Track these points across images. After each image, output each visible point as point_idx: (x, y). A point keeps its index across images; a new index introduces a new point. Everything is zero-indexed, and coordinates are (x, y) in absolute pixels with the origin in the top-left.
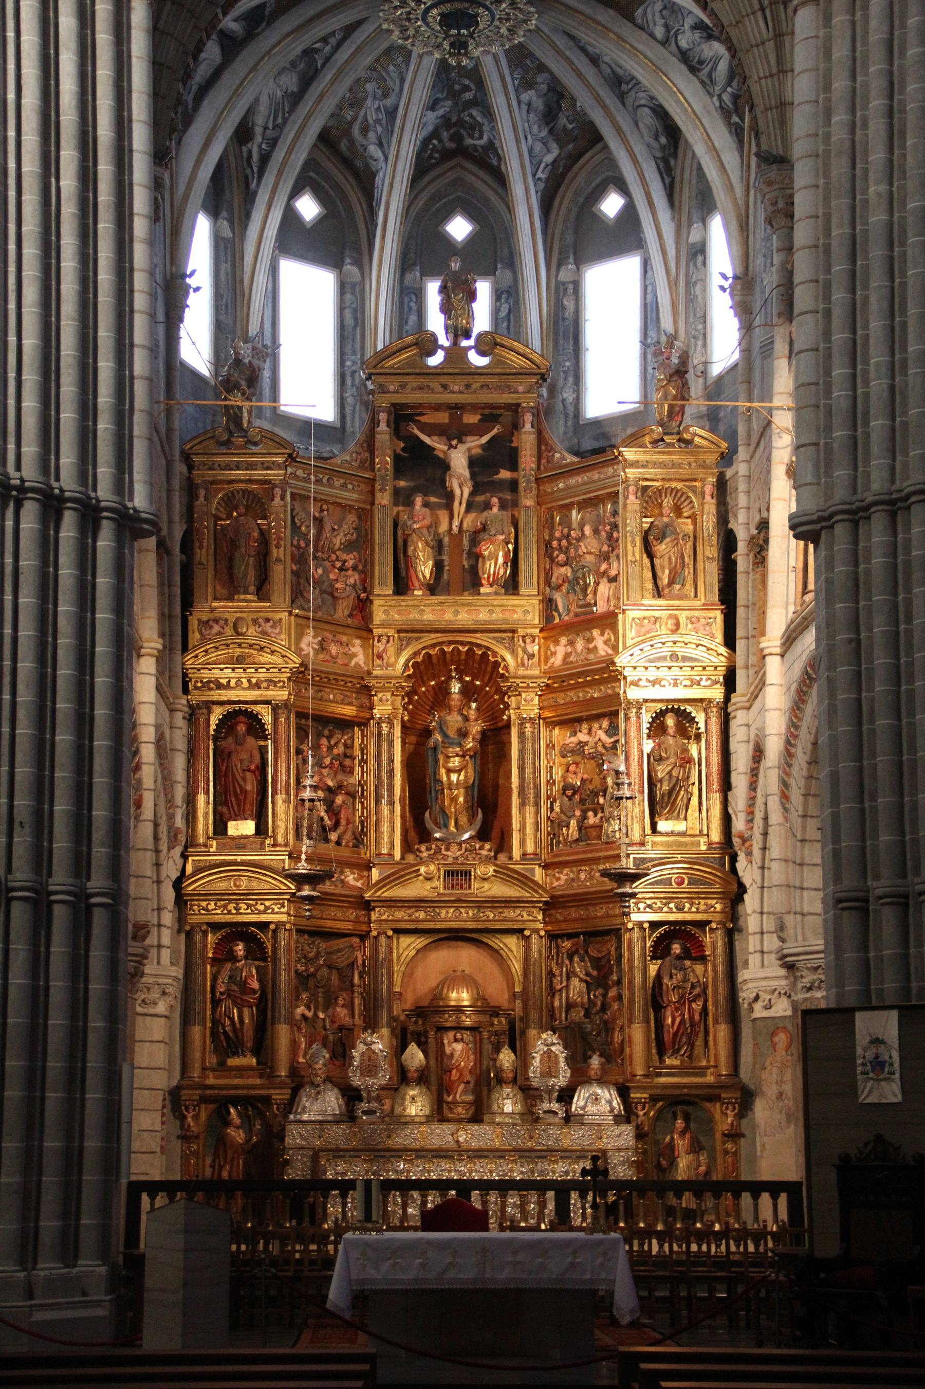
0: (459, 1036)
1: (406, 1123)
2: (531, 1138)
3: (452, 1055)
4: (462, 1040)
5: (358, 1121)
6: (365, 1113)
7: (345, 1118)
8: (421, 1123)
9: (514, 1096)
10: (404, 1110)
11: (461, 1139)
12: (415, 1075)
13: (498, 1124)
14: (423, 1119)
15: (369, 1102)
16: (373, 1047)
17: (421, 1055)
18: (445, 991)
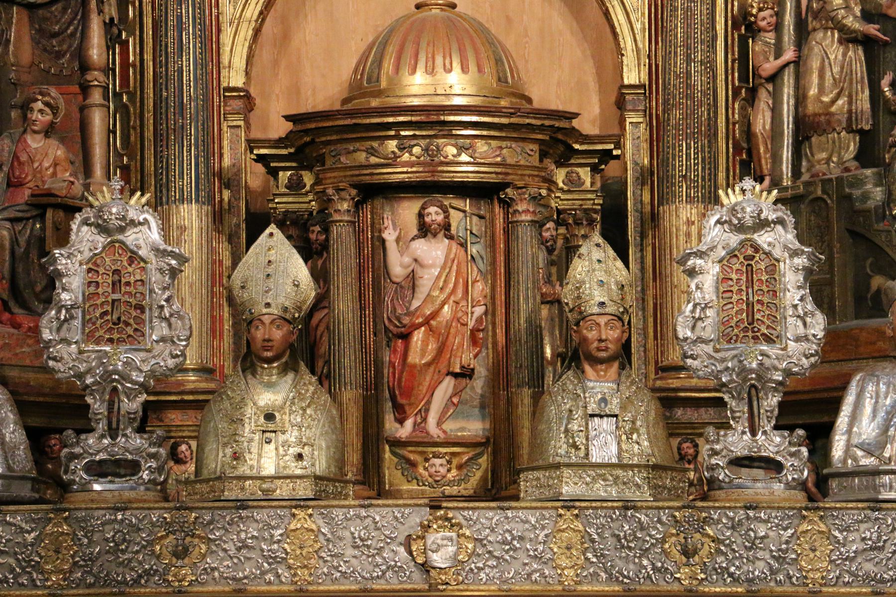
0: (434, 214)
1: (242, 504)
2: (688, 553)
3: (412, 279)
4: (447, 227)
5: (77, 499)
6: (99, 470)
7: (25, 490)
8: (299, 503)
9: (623, 408)
10: (236, 456)
11: (439, 559)
12: (278, 334)
13: (570, 504)
14: (304, 490)
15: (113, 432)
16: (131, 237)
17: (300, 269)
18: (388, 66)
